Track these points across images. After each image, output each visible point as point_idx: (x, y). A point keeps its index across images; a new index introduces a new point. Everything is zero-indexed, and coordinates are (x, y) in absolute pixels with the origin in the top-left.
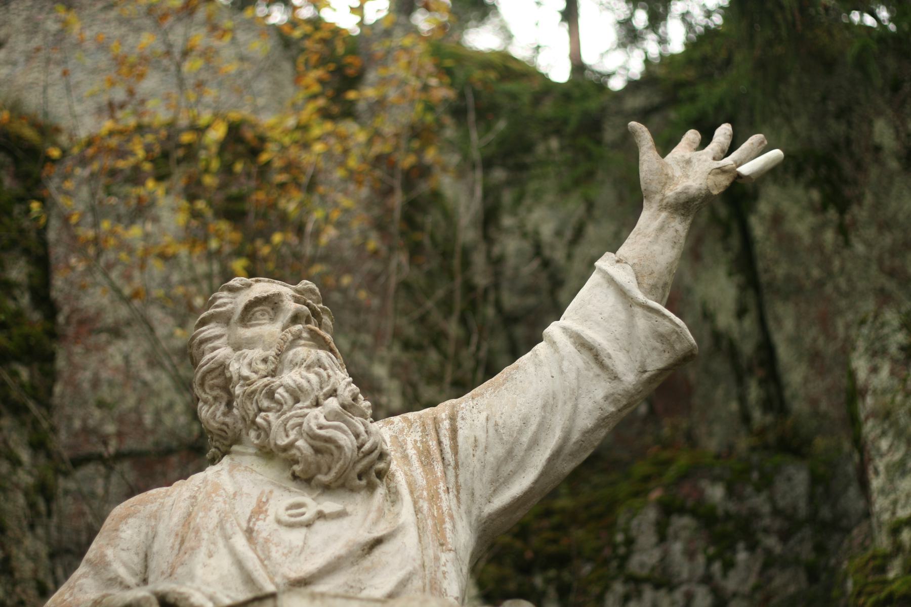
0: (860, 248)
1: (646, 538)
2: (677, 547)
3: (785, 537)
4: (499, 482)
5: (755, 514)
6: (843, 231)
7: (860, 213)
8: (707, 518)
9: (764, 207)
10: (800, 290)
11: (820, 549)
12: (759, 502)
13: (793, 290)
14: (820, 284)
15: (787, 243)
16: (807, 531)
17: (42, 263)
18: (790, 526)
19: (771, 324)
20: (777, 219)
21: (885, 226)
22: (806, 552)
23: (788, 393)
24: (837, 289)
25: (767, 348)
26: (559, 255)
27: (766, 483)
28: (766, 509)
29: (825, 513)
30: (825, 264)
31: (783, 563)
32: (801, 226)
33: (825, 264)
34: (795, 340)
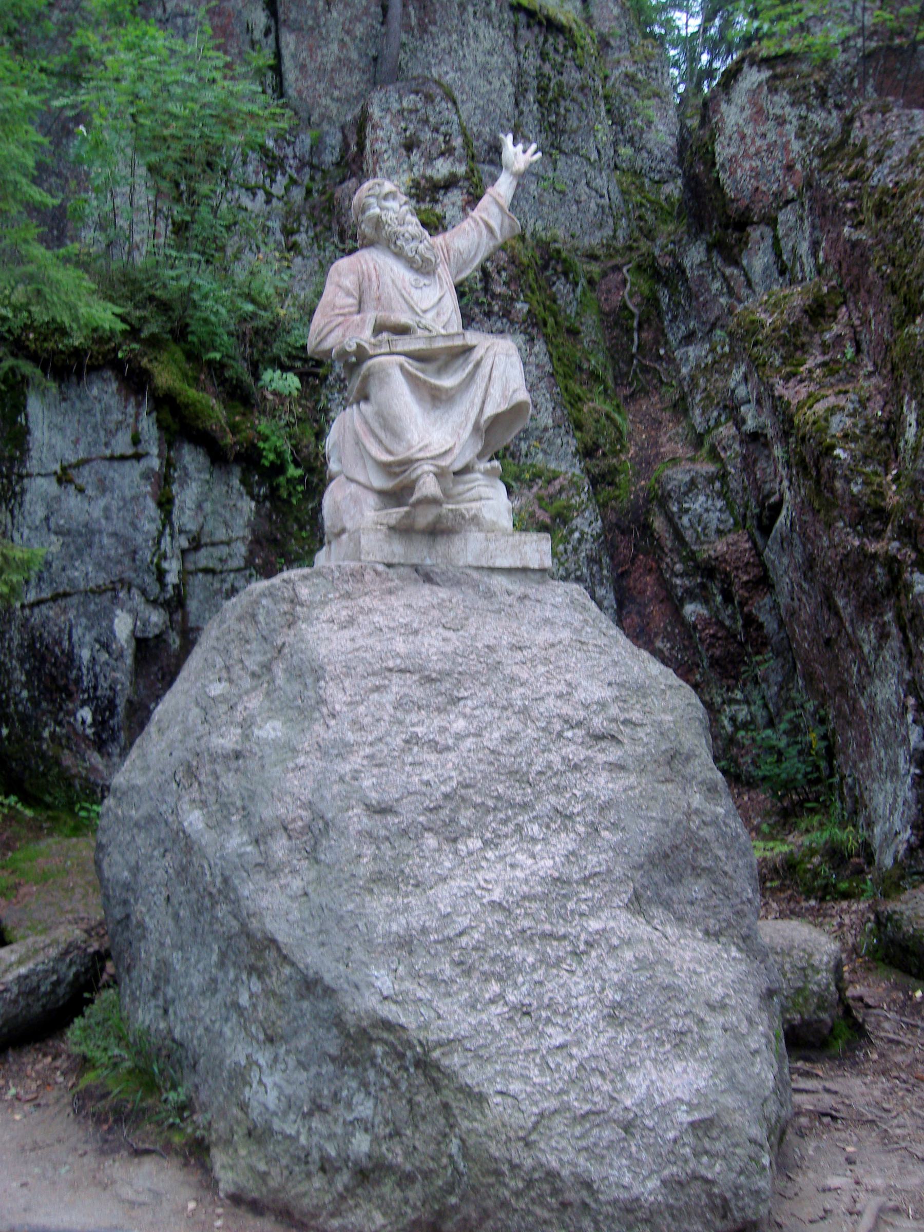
0: (335, 14)
2: (251, 168)
3: (299, 170)
4: (459, 272)
5: (286, 157)
10: (301, 29)
11: (312, 179)
12: (289, 151)
13: (297, 29)
14: (312, 29)
16: (307, 170)
19: (283, 44)
23: (286, 84)
24: (320, 33)
28: (291, 155)
29: (315, 161)
30: (316, 18)
33: (316, 18)
34: (294, 56)
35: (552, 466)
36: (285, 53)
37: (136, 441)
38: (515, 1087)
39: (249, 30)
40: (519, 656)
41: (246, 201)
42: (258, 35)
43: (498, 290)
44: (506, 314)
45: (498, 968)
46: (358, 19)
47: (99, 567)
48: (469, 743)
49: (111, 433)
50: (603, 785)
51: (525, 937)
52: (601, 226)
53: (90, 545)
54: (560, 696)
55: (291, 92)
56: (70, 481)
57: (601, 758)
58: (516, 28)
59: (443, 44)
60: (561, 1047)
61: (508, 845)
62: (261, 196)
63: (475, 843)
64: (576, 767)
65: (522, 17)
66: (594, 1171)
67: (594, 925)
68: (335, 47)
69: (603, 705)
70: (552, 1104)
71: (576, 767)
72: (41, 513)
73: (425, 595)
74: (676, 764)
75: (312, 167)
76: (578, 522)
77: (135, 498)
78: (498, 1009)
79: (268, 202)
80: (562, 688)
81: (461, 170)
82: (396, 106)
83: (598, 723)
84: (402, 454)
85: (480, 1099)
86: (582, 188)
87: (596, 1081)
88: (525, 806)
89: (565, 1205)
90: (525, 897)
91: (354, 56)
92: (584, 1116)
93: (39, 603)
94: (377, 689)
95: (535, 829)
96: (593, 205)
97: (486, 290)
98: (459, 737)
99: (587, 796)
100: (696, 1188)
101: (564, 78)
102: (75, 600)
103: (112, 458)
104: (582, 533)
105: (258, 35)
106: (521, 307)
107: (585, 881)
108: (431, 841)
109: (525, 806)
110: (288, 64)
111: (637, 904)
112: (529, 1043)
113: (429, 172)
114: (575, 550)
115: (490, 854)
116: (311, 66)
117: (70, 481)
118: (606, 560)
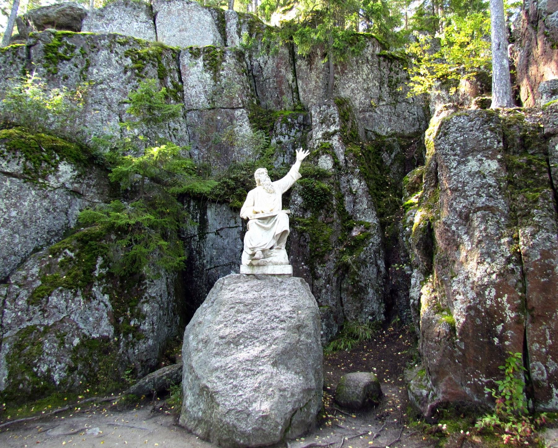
1: (279, 128)
3: (299, 127)
6: (311, 70)
7: (313, 66)
8: (287, 124)
9: (298, 63)
11: (304, 129)
12: (296, 121)
13: (302, 79)
15: (301, 70)
17: (179, 72)
18: (300, 125)
20: (300, 66)
21: (317, 69)
22: (302, 129)
25: (297, 88)
26: (263, 66)
27: (297, 119)
30: (307, 75)
31: (299, 131)
32: (304, 67)
33: (307, 75)
35: (367, 221)
36: (299, 87)
37: (236, 223)
38: (227, 403)
39: (288, 81)
40: (272, 299)
41: (282, 139)
42: (290, 82)
43: (349, 166)
44: (352, 173)
45: (234, 376)
46: (321, 73)
47: (226, 258)
48: (249, 322)
49: (229, 221)
50: (278, 333)
51: (243, 369)
52: (414, 126)
53: (224, 252)
54: (277, 310)
55: (301, 99)
56: (218, 234)
57: (281, 326)
58: (379, 63)
59: (350, 76)
60: (241, 395)
61: (249, 347)
62: (287, 137)
63: (242, 346)
64: (273, 329)
65: (382, 59)
66: (238, 424)
67: (261, 368)
68: (314, 83)
69: (286, 312)
70: (233, 408)
71: (273, 329)
72: (211, 243)
73: (256, 282)
74: (301, 329)
75: (304, 125)
76: (372, 240)
77: (236, 239)
78: (231, 385)
79: (289, 138)
80: (279, 307)
81: (338, 128)
82: (318, 110)
83: (283, 317)
84: (254, 246)
85: (219, 405)
86: (406, 114)
87: (245, 404)
88: (257, 338)
89: (230, 431)
90: (247, 360)
91: (321, 84)
92: (239, 411)
93: (210, 269)
94: (232, 308)
95: (258, 344)
96: (411, 119)
97: (346, 166)
98: (248, 320)
99: (273, 336)
100: (260, 432)
101: (399, 76)
102: (219, 268)
103: (230, 228)
104: (373, 243)
105: (290, 82)
106: (358, 170)
107: (263, 357)
108: (232, 345)
109: (257, 338)
110: (300, 90)
111: (274, 364)
112: (234, 394)
113: (328, 130)
114: (370, 249)
115: (245, 349)
116: (307, 90)
117: (218, 234)
118: (382, 252)
